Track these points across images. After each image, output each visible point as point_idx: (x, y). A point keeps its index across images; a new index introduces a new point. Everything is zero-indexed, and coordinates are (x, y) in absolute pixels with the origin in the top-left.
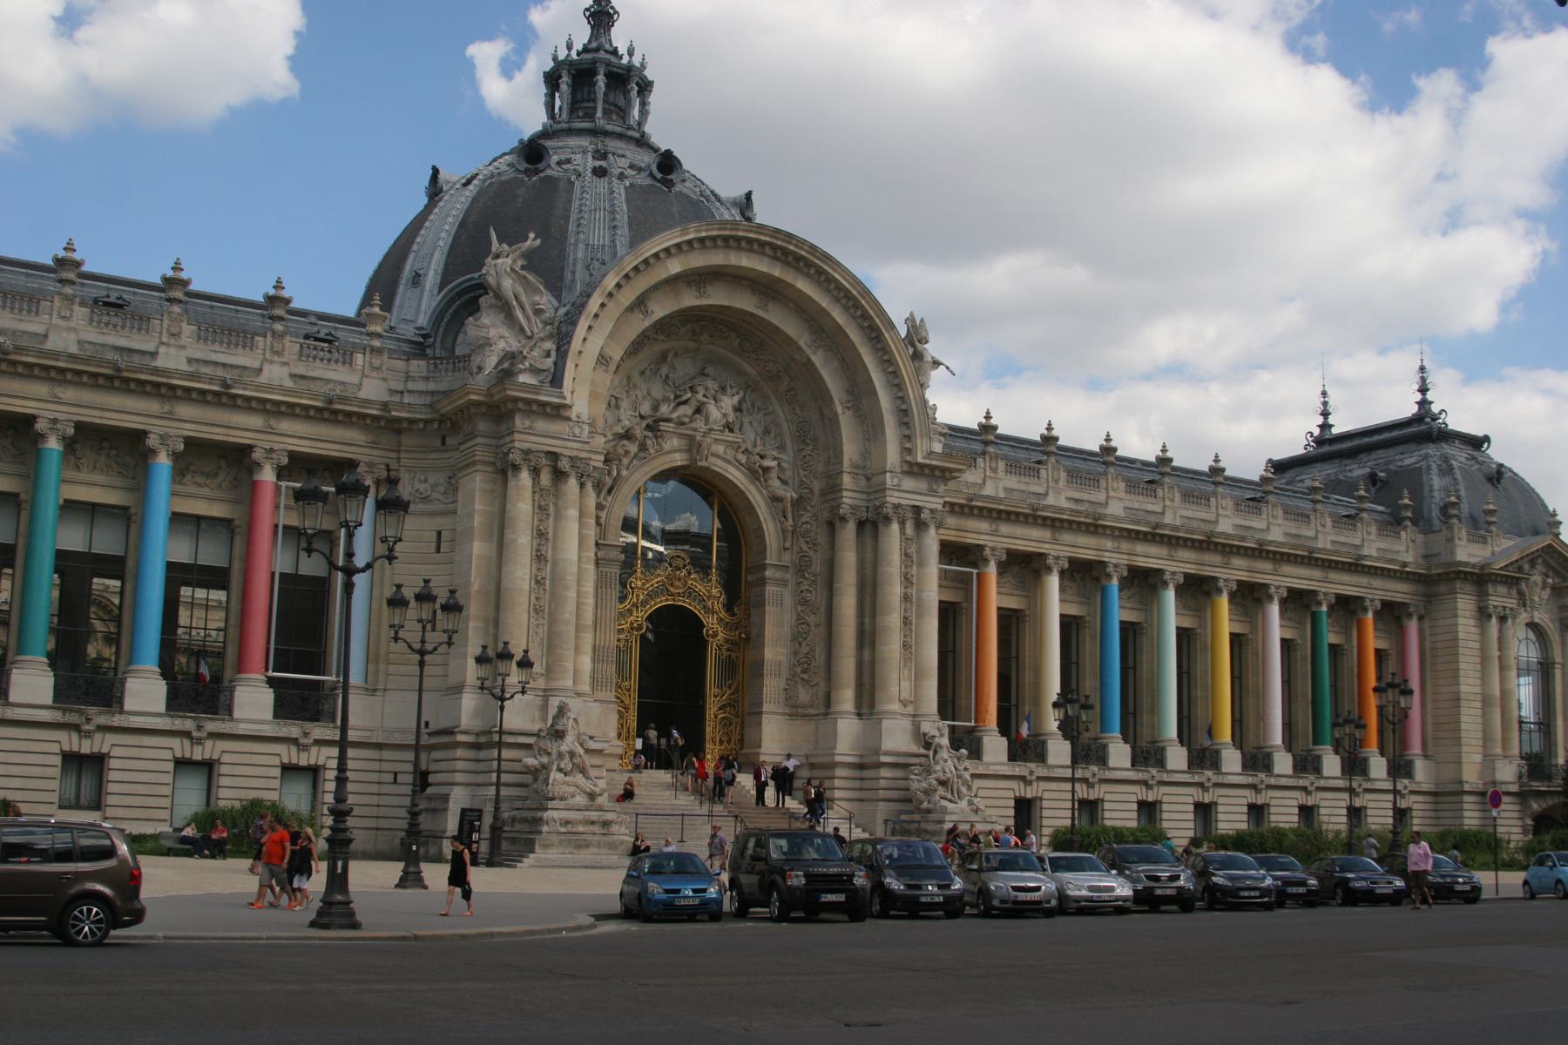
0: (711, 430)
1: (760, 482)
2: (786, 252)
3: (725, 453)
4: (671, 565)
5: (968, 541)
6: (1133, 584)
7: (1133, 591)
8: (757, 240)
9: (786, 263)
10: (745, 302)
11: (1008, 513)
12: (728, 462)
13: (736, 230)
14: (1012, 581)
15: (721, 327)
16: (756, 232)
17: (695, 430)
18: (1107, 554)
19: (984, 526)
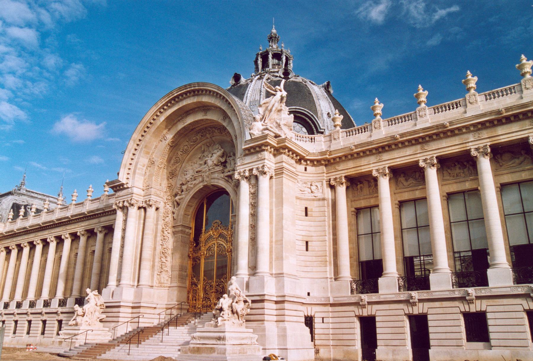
0: (209, 170)
1: (229, 182)
2: (194, 91)
3: (218, 176)
4: (214, 226)
5: (363, 171)
6: (521, 154)
7: (522, 158)
8: (183, 93)
9: (197, 95)
10: (199, 117)
11: (383, 147)
12: (219, 179)
13: (173, 95)
14: (414, 182)
15: (209, 129)
16: (180, 91)
17: (204, 172)
18: (470, 144)
19: (372, 159)
